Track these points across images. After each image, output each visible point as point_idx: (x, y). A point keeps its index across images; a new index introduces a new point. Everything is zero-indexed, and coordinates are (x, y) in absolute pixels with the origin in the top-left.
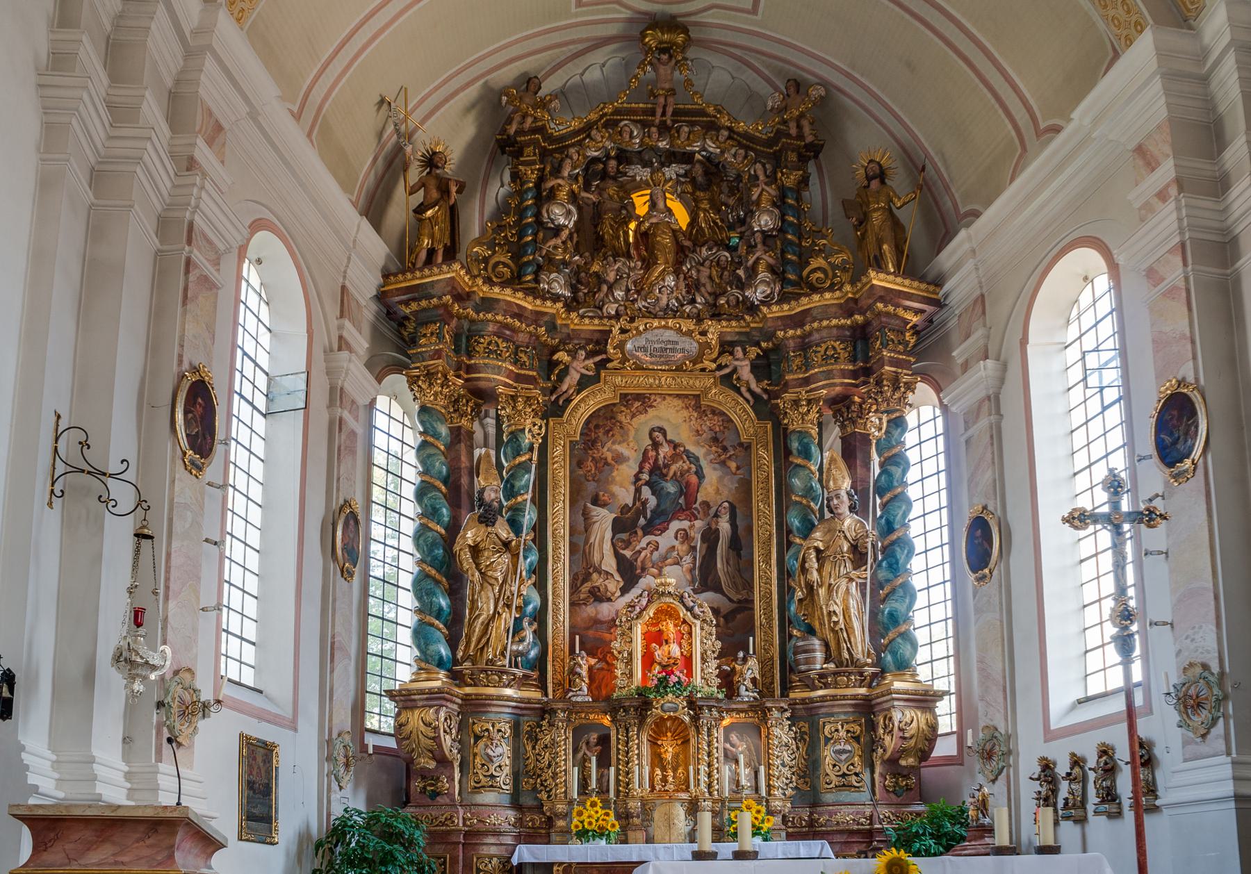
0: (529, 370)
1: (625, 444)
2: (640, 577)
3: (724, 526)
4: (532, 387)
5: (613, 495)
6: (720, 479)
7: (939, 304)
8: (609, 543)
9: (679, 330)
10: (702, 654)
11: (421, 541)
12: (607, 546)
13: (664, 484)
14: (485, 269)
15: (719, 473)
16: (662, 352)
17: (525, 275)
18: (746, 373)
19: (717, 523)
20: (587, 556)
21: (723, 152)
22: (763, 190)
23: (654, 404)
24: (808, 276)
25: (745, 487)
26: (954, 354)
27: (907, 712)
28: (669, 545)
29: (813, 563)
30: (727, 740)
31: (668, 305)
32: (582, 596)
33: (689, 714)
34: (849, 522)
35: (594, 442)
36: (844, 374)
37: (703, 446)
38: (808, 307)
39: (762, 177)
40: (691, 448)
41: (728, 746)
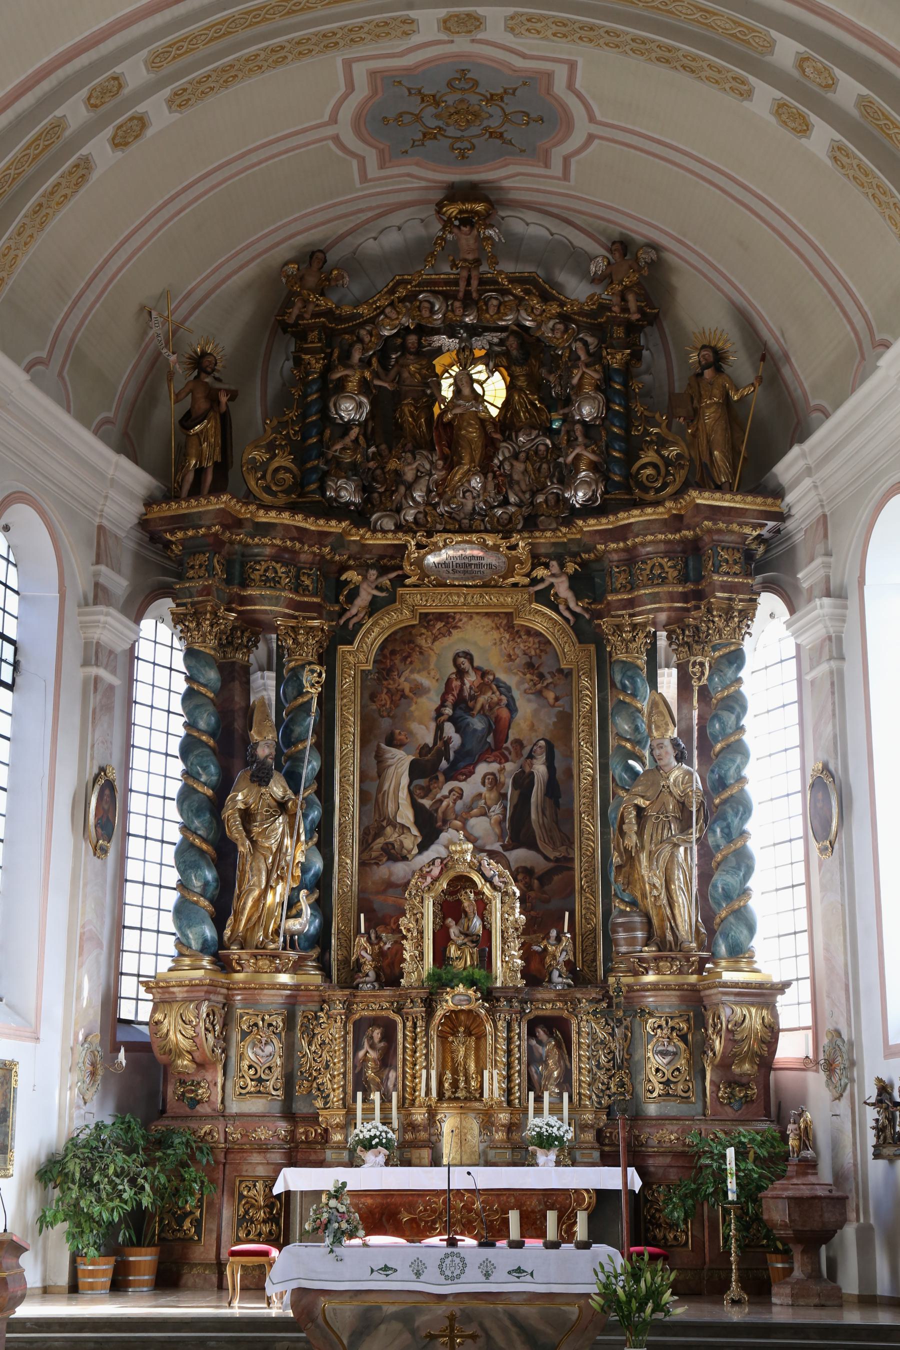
0: (312, 595)
1: (425, 673)
2: (441, 831)
3: (540, 769)
4: (315, 615)
5: (410, 733)
6: (536, 712)
7: (781, 517)
8: (406, 791)
9: (484, 546)
10: (502, 932)
11: (185, 806)
12: (404, 794)
13: (469, 719)
14: (263, 477)
15: (534, 706)
16: (465, 567)
17: (309, 484)
18: (562, 588)
19: (531, 765)
20: (380, 806)
21: (539, 326)
22: (584, 373)
23: (460, 624)
24: (638, 472)
25: (565, 721)
26: (800, 576)
27: (738, 1010)
28: (475, 792)
29: (631, 826)
30: (531, 1034)
31: (474, 509)
32: (374, 854)
33: (483, 1007)
34: (676, 773)
35: (389, 671)
36: (672, 597)
37: (516, 674)
38: (626, 522)
39: (583, 357)
40: (502, 676)
41: (534, 1042)
